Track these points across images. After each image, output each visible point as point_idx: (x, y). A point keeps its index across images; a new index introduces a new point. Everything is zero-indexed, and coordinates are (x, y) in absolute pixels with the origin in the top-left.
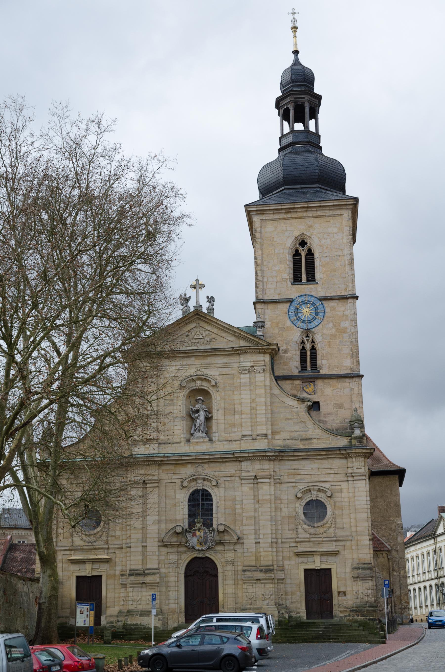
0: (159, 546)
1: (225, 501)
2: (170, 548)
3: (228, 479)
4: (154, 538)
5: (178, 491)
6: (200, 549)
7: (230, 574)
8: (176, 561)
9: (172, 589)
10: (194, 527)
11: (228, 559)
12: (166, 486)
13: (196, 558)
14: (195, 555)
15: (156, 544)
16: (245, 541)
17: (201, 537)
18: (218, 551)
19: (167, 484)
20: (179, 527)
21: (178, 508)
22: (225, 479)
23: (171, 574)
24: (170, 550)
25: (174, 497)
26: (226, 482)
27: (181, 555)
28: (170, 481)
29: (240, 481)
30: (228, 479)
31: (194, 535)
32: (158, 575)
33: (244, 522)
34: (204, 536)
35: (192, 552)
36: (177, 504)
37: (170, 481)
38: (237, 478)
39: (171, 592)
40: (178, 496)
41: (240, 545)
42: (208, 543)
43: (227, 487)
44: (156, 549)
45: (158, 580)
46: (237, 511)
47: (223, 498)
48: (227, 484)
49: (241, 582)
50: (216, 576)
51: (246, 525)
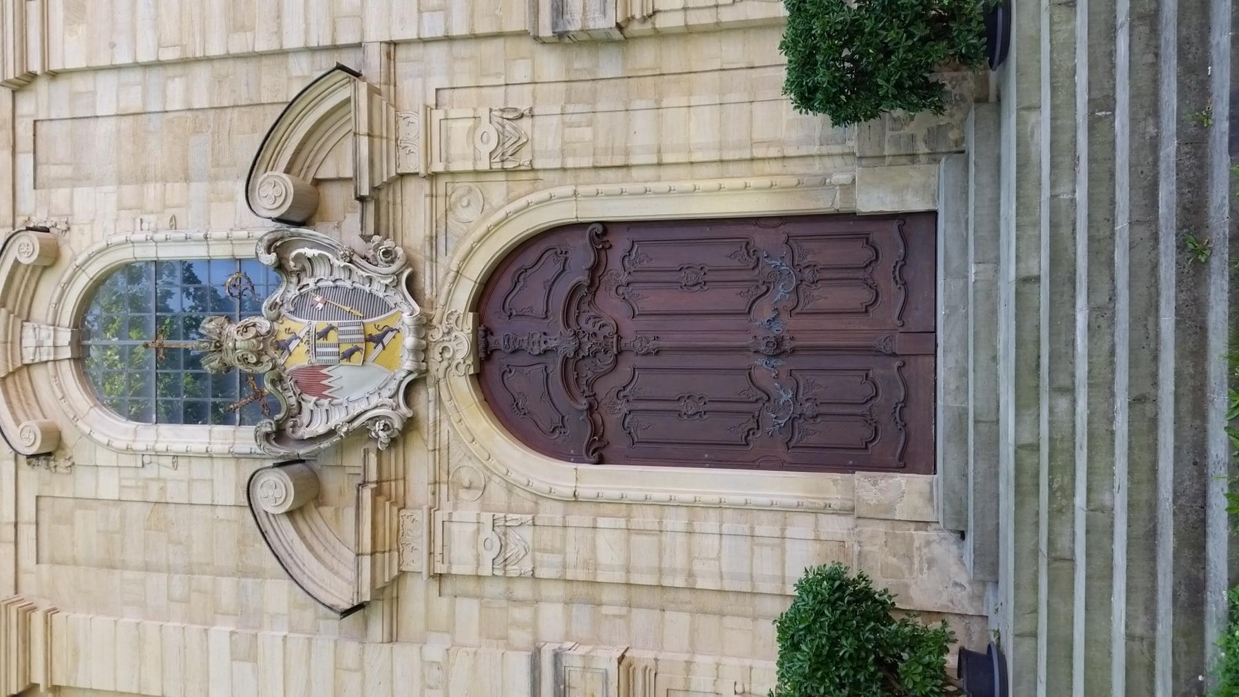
0: (392, 638)
1: (145, 180)
2: (408, 556)
3: (25, 162)
4: (337, 667)
5: (84, 484)
6: (409, 341)
7: (587, 133)
8: (487, 518)
9: (680, 561)
10: (258, 378)
11: (485, 150)
12: (54, 562)
13: (479, 378)
14: (462, 387)
15: (377, 654)
16: (375, 33)
17: (324, 334)
18: (433, 221)
19: (45, 554)
20: (259, 493)
21: (175, 493)
22: (26, 181)
23: (571, 558)
24: (416, 561)
25: (115, 513)
26: (43, 171)
27: (454, 485)
28: (27, 532)
29: (42, 86)
30: (25, 162)
31: (313, 381)
32: (573, 662)
33: (261, 47)
34: (321, 315)
35: (439, 400)
36: (154, 497)
37: (27, 532)
38: (28, 105)
39: (698, 567)
40: (108, 487)
41: (402, 68)
42: (377, 289)
43: (68, 171)
44: (405, 655)
45: (606, 659)
46: (201, 101)
47: (129, 190)
48: (54, 171)
49: (646, 56)
50: (602, 233)
51: (279, 33)
